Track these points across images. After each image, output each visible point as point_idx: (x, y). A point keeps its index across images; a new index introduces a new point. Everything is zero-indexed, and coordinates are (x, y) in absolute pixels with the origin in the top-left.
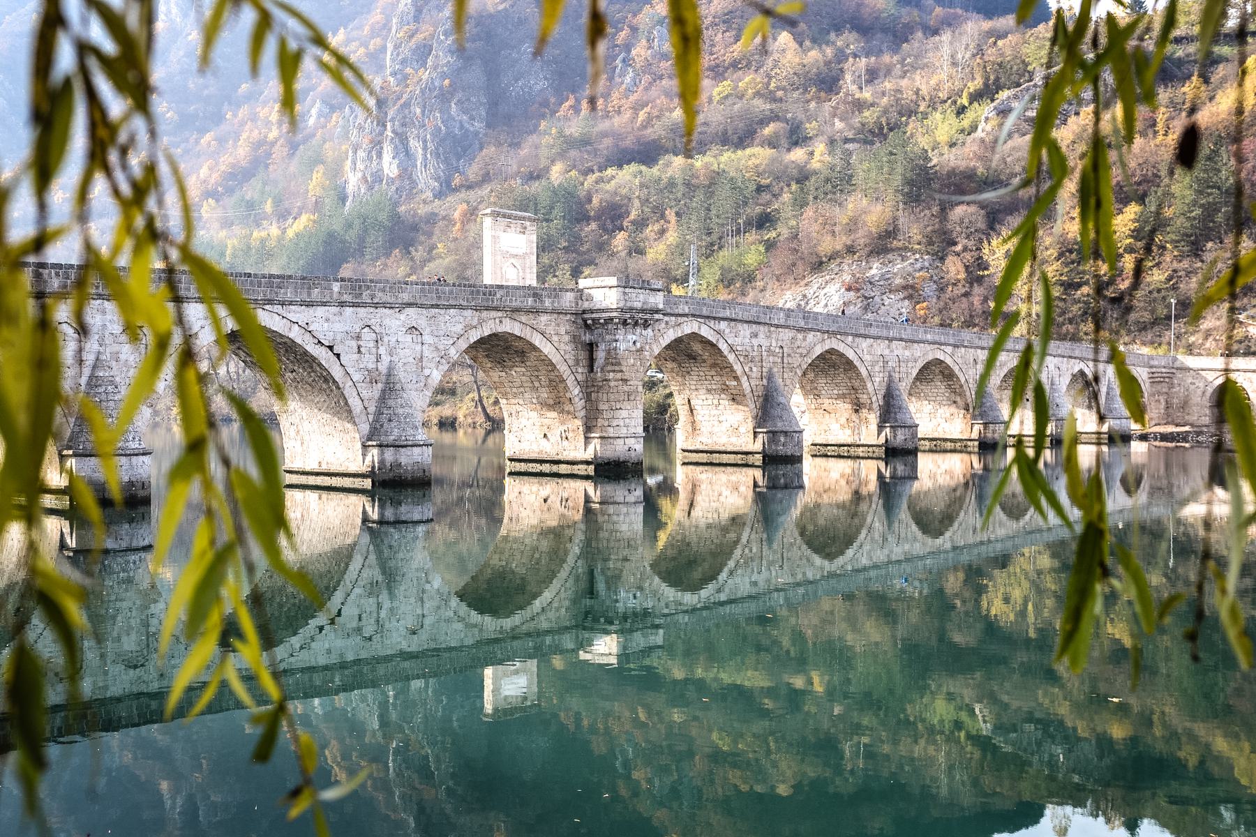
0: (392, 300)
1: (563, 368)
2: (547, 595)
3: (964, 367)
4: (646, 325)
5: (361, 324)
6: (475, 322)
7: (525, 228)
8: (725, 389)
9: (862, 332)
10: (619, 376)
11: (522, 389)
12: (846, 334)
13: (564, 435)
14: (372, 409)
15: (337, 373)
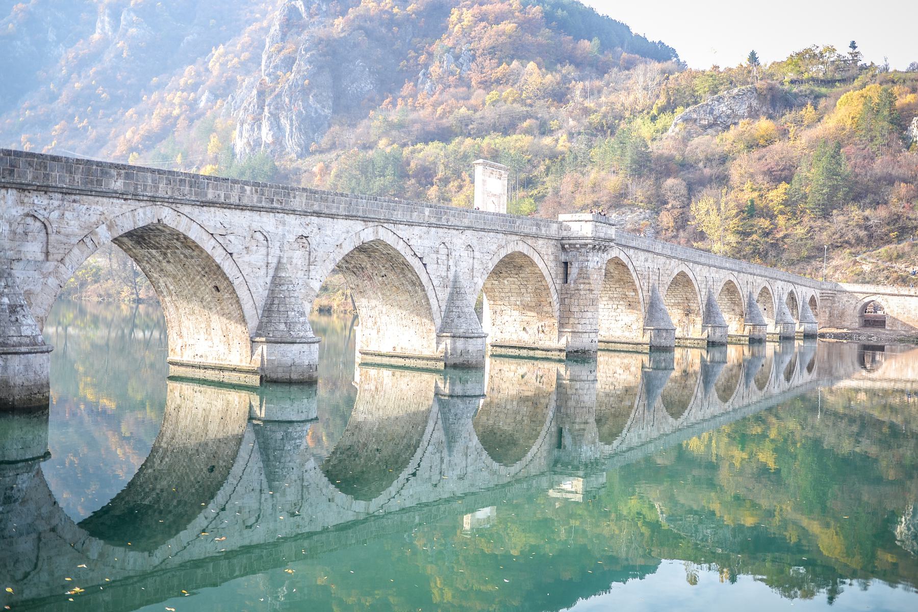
0: (459, 224)
1: (549, 279)
2: (534, 449)
3: (742, 286)
4: (604, 251)
5: (439, 241)
6: (503, 243)
7: (501, 175)
8: (625, 297)
9: (697, 260)
10: (587, 287)
11: (510, 294)
12: (689, 261)
13: (540, 329)
14: (443, 308)
15: (424, 279)
